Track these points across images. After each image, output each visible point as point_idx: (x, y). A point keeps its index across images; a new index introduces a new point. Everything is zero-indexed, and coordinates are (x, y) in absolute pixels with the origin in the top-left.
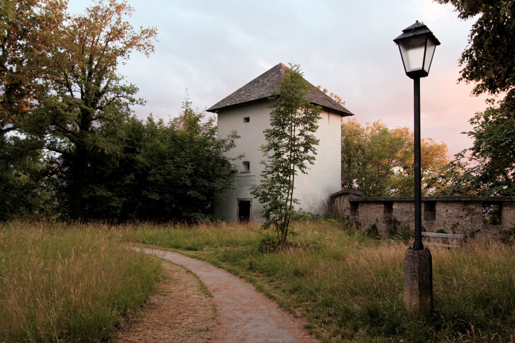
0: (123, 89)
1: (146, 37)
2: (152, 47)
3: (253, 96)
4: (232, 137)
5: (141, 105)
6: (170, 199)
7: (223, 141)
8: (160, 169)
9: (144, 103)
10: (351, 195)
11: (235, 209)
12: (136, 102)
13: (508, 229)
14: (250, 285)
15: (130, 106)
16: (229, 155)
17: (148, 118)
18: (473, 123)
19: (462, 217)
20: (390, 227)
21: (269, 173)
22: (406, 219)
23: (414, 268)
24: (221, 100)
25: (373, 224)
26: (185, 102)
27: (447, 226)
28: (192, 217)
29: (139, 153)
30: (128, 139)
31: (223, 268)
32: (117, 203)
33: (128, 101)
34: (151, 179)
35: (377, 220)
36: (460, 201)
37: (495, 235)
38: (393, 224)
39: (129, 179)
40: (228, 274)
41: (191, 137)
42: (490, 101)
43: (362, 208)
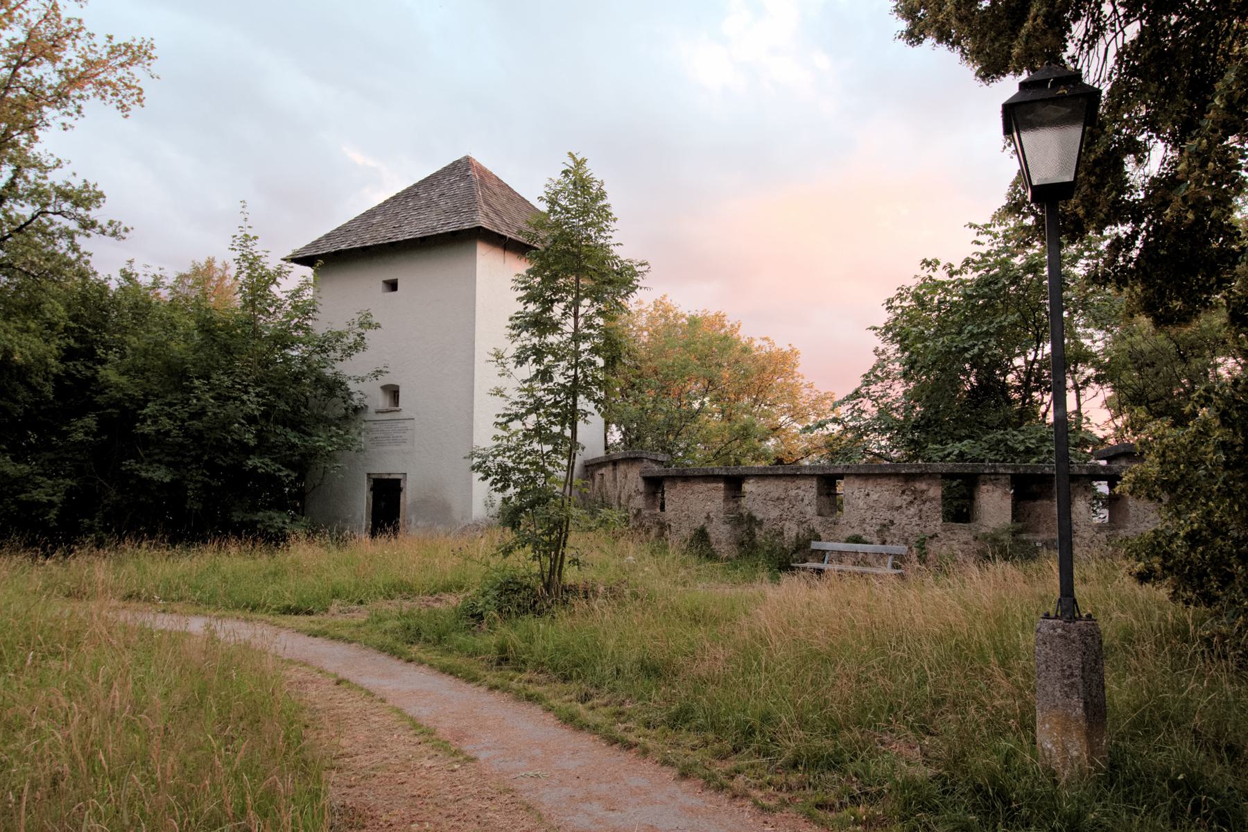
0: (66, 196)
1: (122, 65)
2: (136, 91)
3: (407, 228)
4: (361, 325)
5: (113, 239)
6: (199, 478)
7: (340, 336)
8: (170, 405)
9: (123, 234)
10: (645, 463)
11: (362, 502)
12: (98, 229)
13: (989, 531)
14: (537, 710)
15: (79, 240)
16: (350, 368)
17: (123, 271)
18: (891, 308)
19: (901, 507)
20: (739, 531)
21: (518, 416)
22: (775, 513)
23: (1070, 667)
24: (322, 235)
25: (697, 526)
26: (240, 235)
27: (868, 528)
28: (257, 522)
29: (103, 362)
30: (73, 325)
31: (421, 663)
32: (48, 491)
33: (73, 225)
34: (147, 430)
35: (708, 517)
36: (897, 475)
37: (966, 543)
38: (745, 527)
39: (83, 428)
40: (446, 681)
41: (251, 322)
42: (929, 264)
43: (672, 491)
